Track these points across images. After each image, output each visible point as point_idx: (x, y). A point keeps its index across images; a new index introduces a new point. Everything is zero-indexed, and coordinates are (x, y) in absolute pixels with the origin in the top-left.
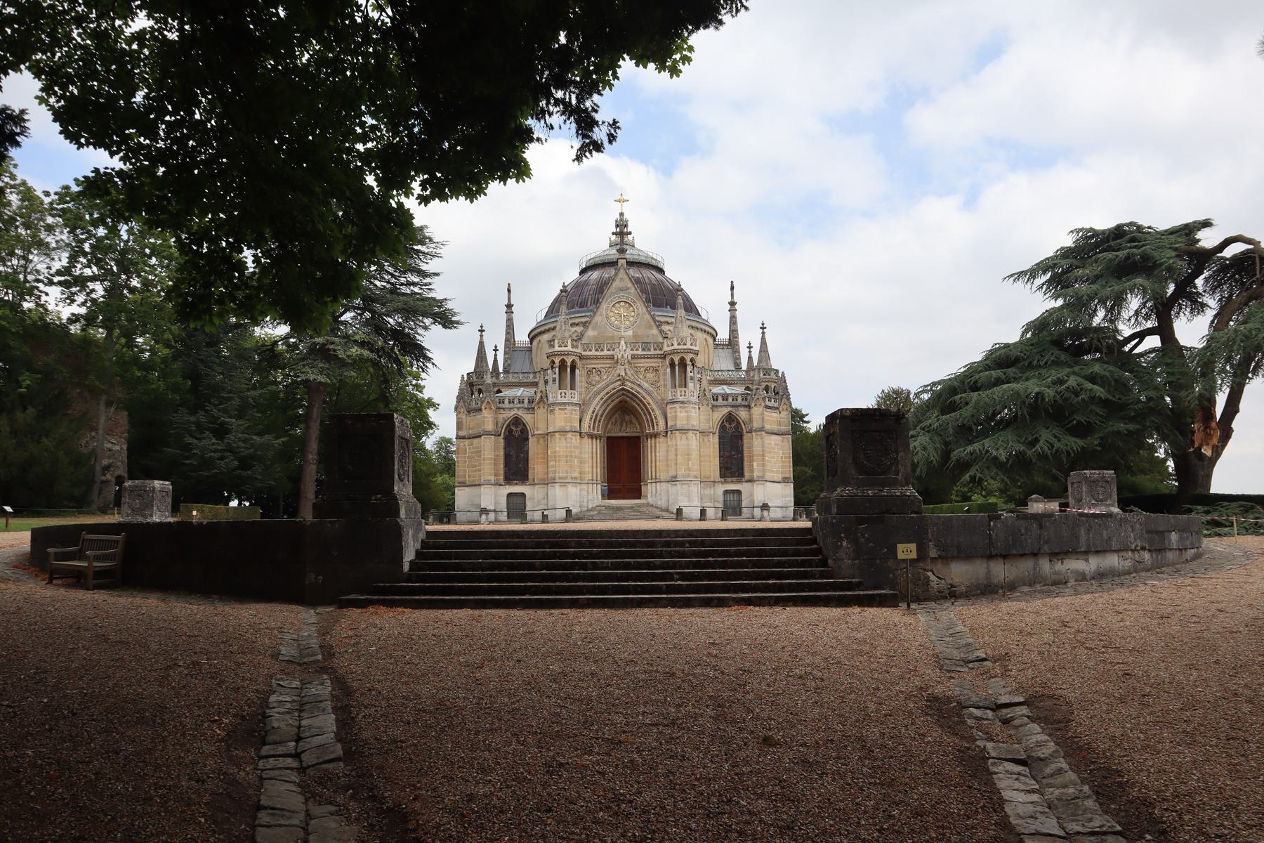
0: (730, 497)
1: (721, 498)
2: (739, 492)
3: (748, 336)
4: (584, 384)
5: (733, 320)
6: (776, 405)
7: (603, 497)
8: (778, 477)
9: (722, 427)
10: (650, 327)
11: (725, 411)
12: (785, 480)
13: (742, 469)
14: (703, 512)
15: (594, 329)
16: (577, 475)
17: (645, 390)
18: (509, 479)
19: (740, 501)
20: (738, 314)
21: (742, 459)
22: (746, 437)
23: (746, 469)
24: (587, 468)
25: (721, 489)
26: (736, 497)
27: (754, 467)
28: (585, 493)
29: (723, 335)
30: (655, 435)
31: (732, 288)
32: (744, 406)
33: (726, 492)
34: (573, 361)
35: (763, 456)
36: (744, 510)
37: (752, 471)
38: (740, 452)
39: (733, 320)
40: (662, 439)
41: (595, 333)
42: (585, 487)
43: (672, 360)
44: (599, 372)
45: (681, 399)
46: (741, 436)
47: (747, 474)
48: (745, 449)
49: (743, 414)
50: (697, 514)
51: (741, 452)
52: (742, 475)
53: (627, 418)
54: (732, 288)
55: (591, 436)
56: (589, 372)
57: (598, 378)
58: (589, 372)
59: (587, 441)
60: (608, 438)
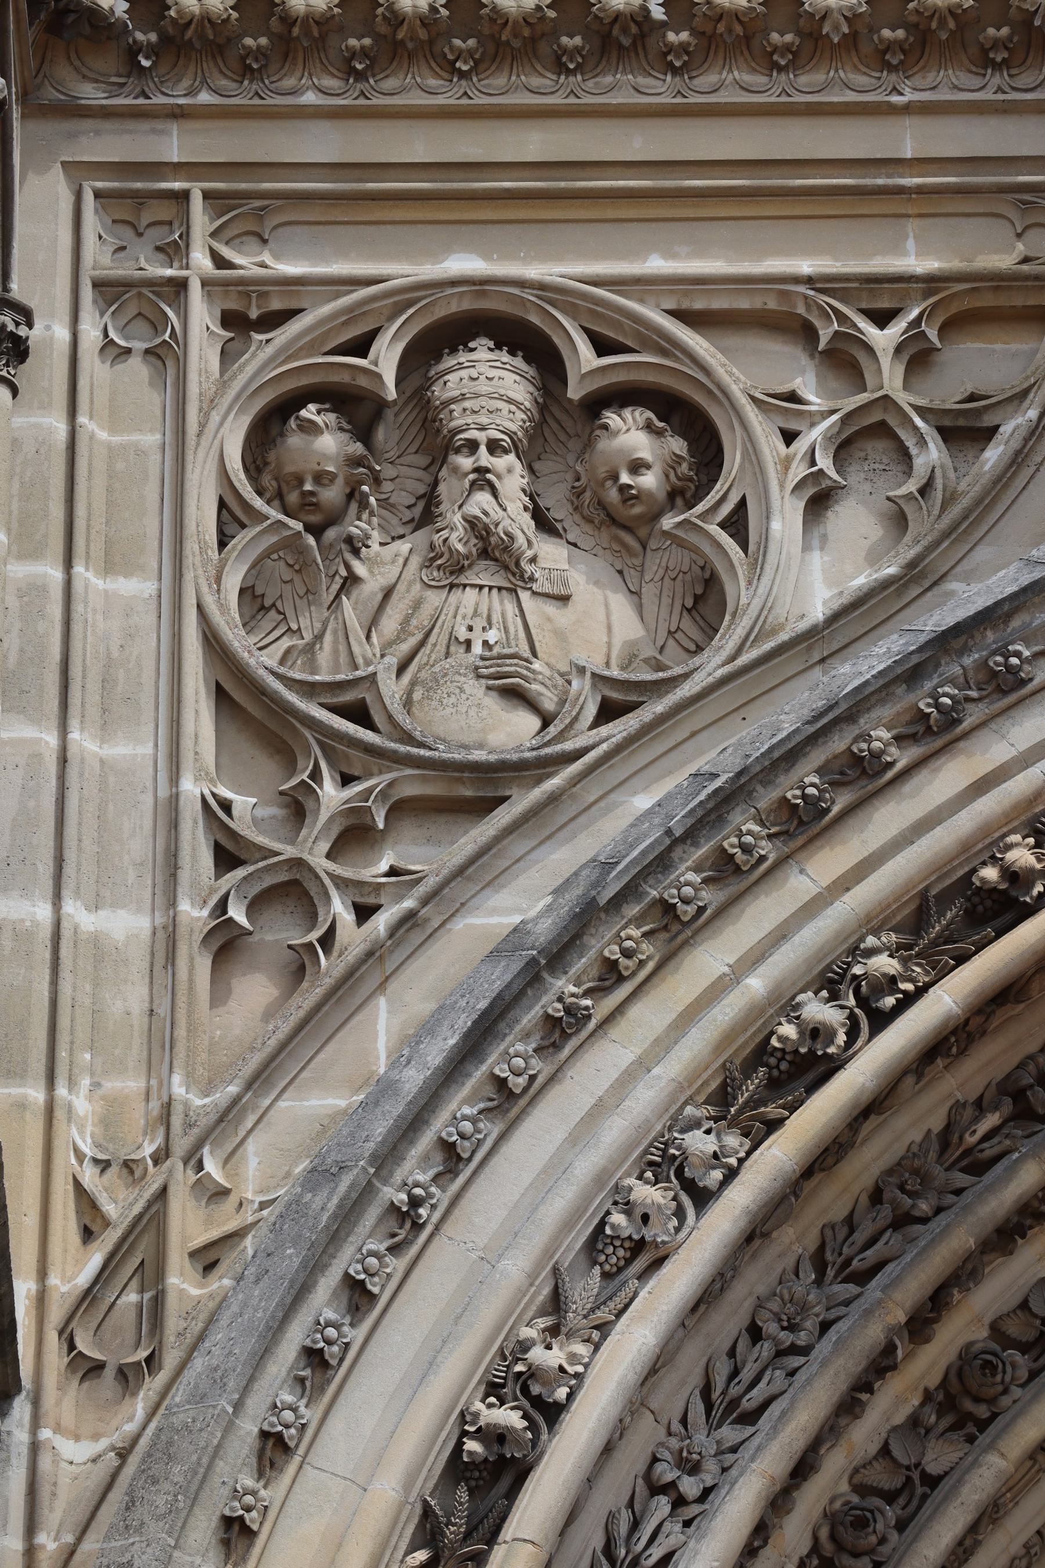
57: (591, 616)
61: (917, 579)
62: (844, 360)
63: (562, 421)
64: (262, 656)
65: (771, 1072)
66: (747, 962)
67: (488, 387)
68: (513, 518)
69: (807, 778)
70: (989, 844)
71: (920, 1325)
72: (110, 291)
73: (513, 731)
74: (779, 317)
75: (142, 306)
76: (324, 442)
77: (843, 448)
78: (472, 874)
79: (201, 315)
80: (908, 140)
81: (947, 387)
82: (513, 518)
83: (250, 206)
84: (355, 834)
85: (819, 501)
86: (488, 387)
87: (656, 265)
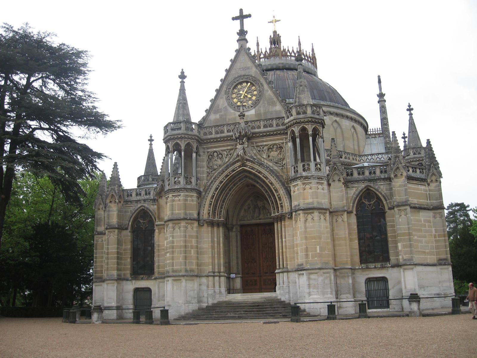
0: (374, 286)
1: (363, 287)
2: (384, 280)
3: (399, 127)
4: (205, 169)
5: (383, 110)
6: (423, 176)
7: (230, 290)
8: (433, 259)
9: (360, 206)
10: (273, 104)
11: (362, 186)
12: (441, 263)
13: (388, 252)
14: (331, 308)
15: (215, 113)
16: (194, 267)
17: (267, 168)
18: (136, 274)
19: (387, 290)
20: (387, 104)
21: (385, 242)
22: (389, 213)
23: (391, 252)
24: (207, 259)
25: (362, 278)
26: (381, 285)
27: (400, 250)
28: (204, 288)
29: (374, 124)
30: (281, 218)
31: (380, 82)
32: (384, 179)
33: (369, 281)
34: (188, 145)
35: (409, 234)
36: (392, 302)
37: (397, 254)
38: (382, 231)
39: (383, 110)
40: (287, 222)
41: (218, 116)
42: (204, 280)
43: (293, 132)
44: (220, 154)
45: (304, 174)
46: (382, 214)
47: (392, 258)
48: (389, 229)
49: (382, 188)
50: (325, 312)
51: (385, 233)
52: (387, 259)
53: (260, 204)
54: (380, 82)
55: (212, 224)
56: (211, 157)
57: (219, 162)
58: (211, 157)
59: (206, 231)
60: (242, 226)
61: (229, 160)
62: (227, 152)
63: (218, 155)
64: (208, 165)
65: (221, 182)
66: (221, 179)
67: (215, 154)
68: (216, 159)
69: (222, 172)
70: (228, 174)
71: (228, 188)
72: (203, 152)
73: (216, 167)
74: (225, 150)
75: (204, 152)
76: (210, 157)
77: (227, 156)
78: (215, 172)
79: (206, 153)
80: (228, 144)
81: (230, 153)
82: (216, 159)
83: (208, 148)
84: (212, 172)
85: (226, 158)
86: (215, 154)
87: (221, 149)
